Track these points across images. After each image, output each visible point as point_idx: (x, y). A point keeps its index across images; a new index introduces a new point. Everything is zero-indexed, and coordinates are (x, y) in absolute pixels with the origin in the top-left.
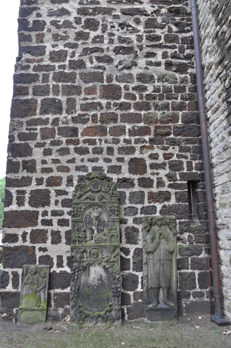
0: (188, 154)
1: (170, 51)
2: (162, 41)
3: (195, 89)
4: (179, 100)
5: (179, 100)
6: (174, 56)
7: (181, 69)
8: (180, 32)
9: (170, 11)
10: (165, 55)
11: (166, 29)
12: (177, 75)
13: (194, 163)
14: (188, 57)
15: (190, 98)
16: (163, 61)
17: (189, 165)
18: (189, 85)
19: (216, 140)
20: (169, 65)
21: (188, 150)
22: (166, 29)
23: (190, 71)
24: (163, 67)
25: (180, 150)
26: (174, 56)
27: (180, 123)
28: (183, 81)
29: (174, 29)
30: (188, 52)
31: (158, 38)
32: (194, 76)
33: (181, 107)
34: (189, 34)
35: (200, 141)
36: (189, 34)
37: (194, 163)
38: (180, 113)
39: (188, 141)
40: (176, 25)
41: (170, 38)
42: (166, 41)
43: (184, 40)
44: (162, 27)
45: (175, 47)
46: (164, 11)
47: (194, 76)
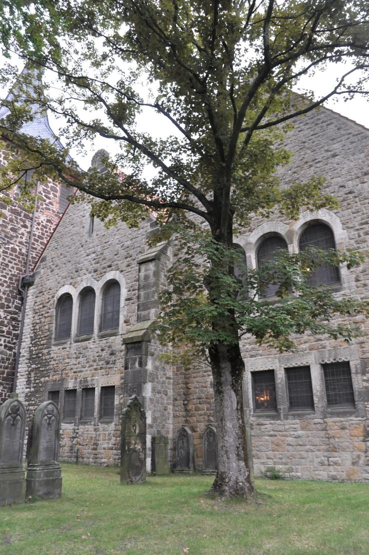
0: (6, 390)
1: (7, 339)
2: (5, 334)
3: (15, 360)
4: (7, 364)
5: (7, 364)
6: (9, 342)
7: (10, 349)
8: (14, 330)
9: (11, 317)
10: (5, 341)
11: (8, 328)
12: (8, 352)
13: (7, 394)
14: (14, 344)
15: (11, 364)
16: (4, 344)
17: (5, 394)
18: (12, 358)
19: (19, 387)
20: (6, 346)
21: (6, 388)
22: (8, 328)
23: (14, 350)
24: (3, 347)
25: (3, 388)
26: (9, 342)
27: (5, 375)
28: (10, 355)
29: (11, 328)
30: (14, 341)
31: (4, 332)
32: (15, 354)
33: (7, 368)
34: (17, 332)
35: (12, 385)
36: (17, 332)
37: (7, 394)
38: (6, 371)
39: (7, 384)
40: (12, 326)
41: (9, 333)
42: (7, 334)
43: (14, 334)
44: (6, 326)
45: (9, 338)
46: (9, 317)
47: (15, 354)
